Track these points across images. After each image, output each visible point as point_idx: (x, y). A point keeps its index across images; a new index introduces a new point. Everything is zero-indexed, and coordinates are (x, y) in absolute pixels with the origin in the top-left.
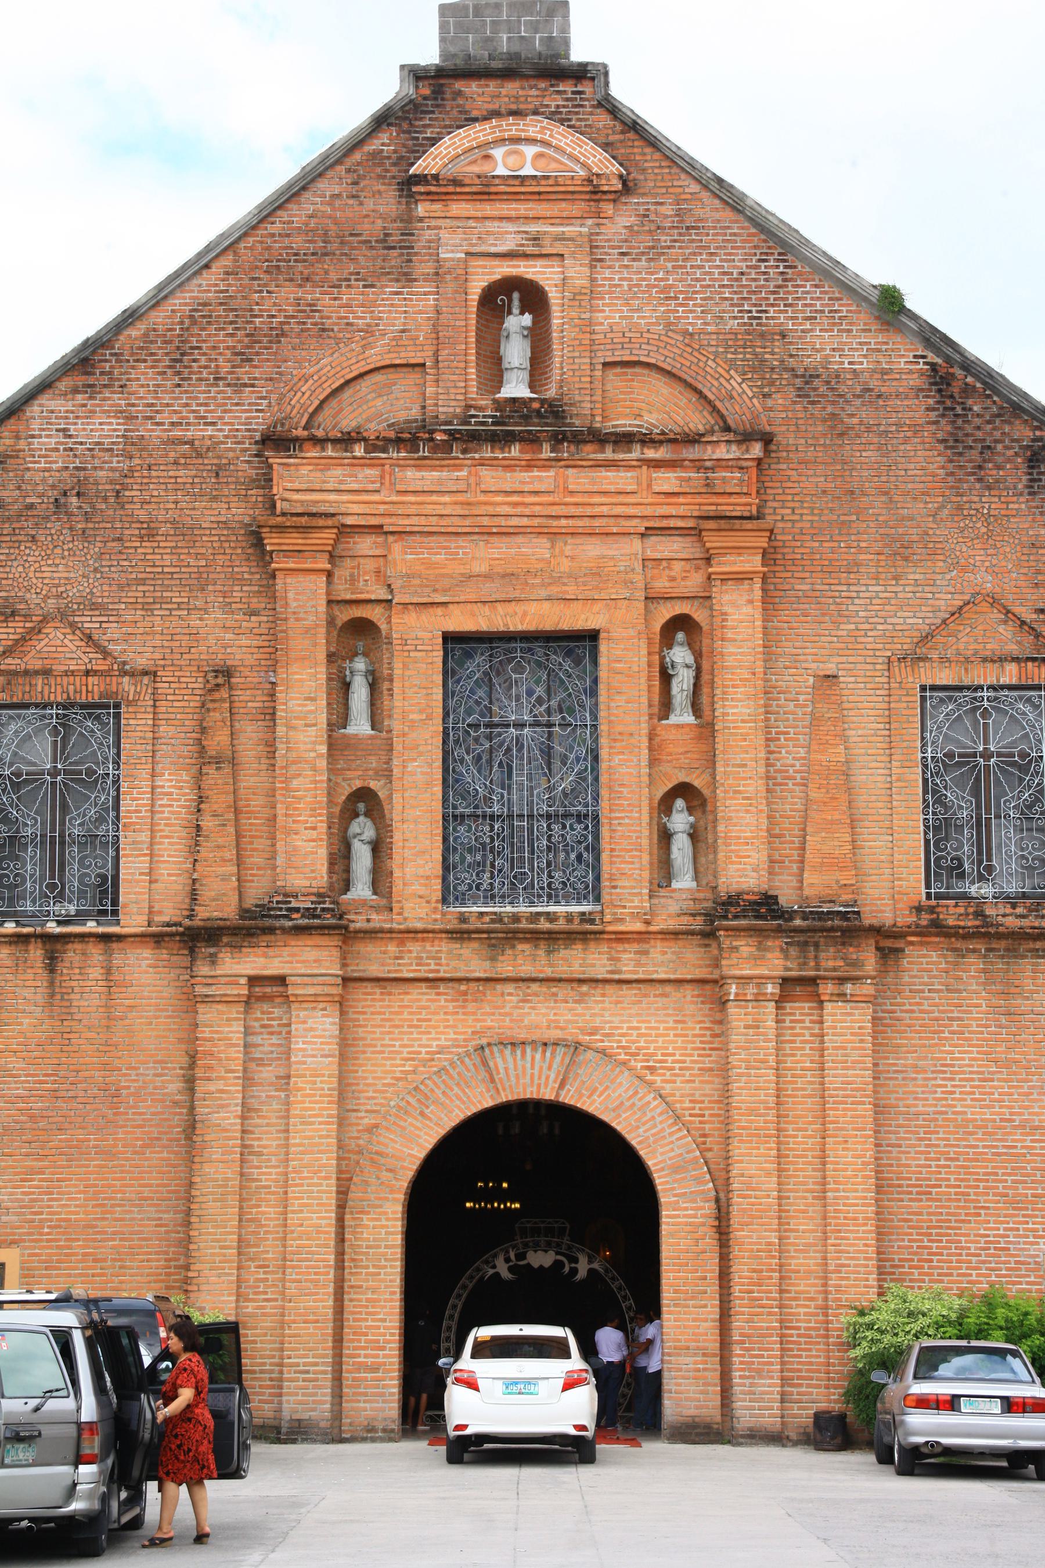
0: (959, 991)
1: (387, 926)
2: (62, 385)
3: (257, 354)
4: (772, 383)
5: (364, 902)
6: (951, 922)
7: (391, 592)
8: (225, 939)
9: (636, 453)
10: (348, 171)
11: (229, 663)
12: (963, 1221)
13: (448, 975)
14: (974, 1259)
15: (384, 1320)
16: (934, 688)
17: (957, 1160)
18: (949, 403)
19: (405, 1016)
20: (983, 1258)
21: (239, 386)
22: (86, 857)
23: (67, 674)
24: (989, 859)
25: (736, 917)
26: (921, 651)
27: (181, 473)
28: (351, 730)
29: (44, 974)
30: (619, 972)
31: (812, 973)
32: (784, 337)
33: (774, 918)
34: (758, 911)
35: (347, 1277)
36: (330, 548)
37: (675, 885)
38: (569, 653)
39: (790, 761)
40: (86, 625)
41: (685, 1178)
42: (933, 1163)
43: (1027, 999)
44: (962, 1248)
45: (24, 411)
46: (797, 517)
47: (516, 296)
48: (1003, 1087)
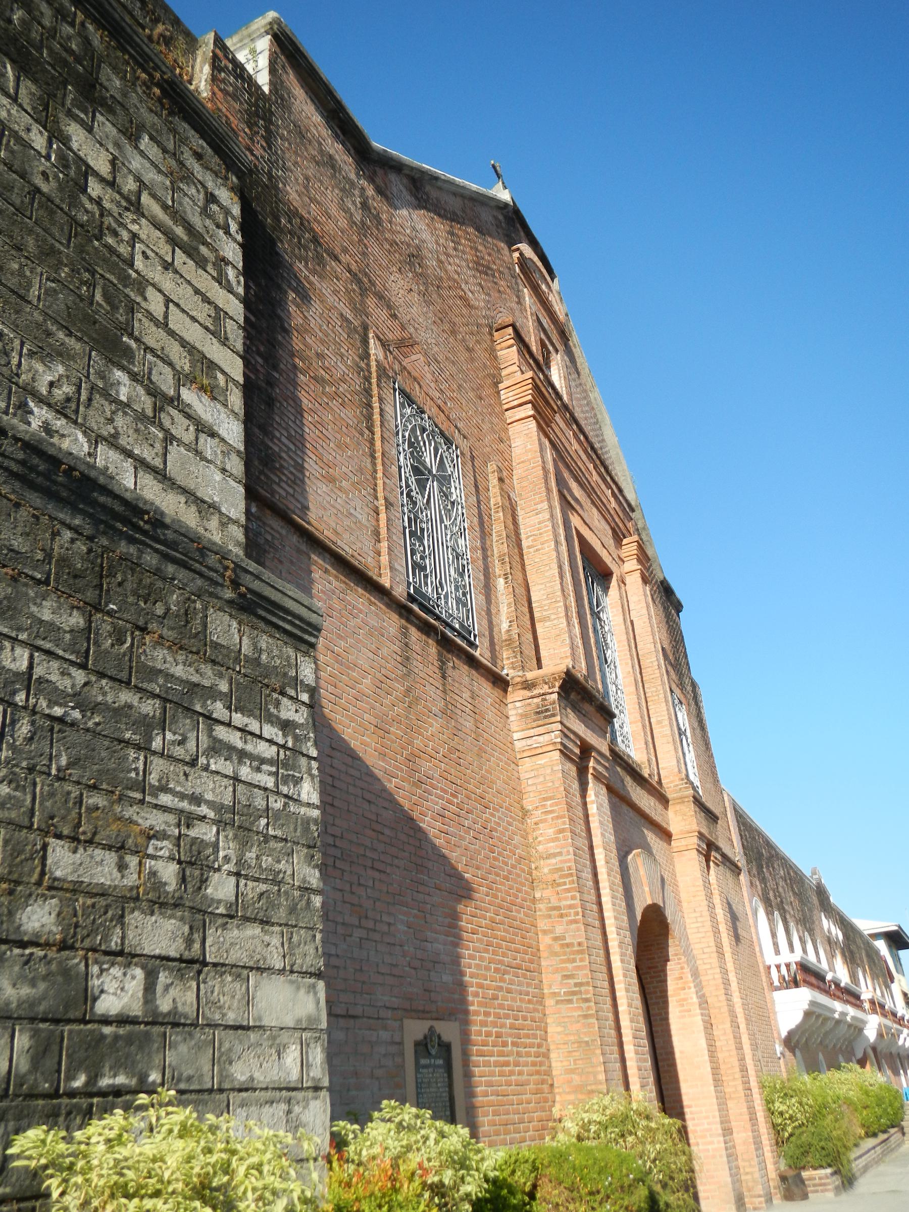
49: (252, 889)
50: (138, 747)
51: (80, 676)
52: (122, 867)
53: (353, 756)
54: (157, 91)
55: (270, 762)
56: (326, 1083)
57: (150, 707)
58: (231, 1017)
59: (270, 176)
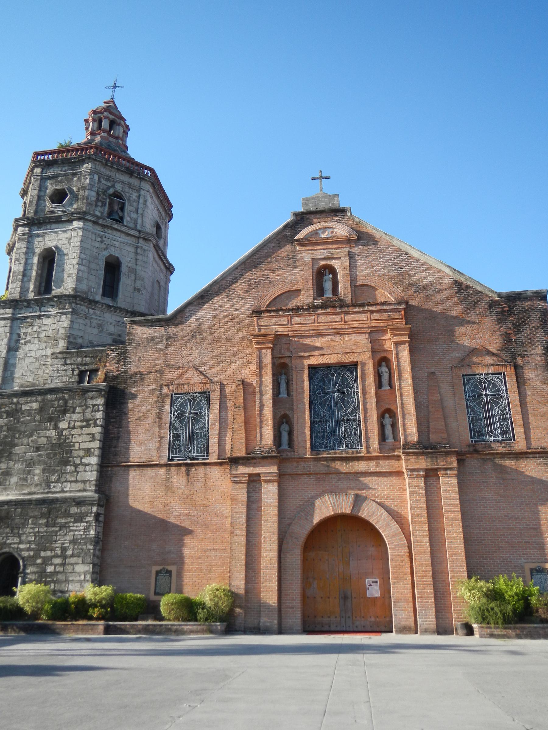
0: (484, 472)
1: (293, 457)
2: (195, 303)
3: (251, 290)
4: (407, 288)
5: (285, 451)
6: (480, 449)
7: (292, 354)
8: (240, 462)
9: (366, 308)
10: (277, 240)
11: (243, 378)
12: (494, 552)
13: (313, 472)
14: (499, 565)
15: (295, 590)
16: (467, 375)
17: (490, 530)
18: (462, 291)
19: (300, 486)
20: (502, 565)
21: (246, 299)
22: (199, 439)
23: (194, 384)
24: (491, 428)
25: (408, 449)
26: (462, 364)
27: (229, 324)
28: (280, 396)
29: (186, 476)
30: (370, 470)
31: (436, 467)
32: (409, 275)
33: (421, 449)
34: (416, 447)
35: (282, 575)
36: (272, 341)
37: (387, 441)
38: (348, 370)
39: (422, 400)
40: (200, 369)
41: (396, 539)
42: (482, 532)
43: (509, 474)
44: (495, 561)
45: (184, 311)
46: (417, 326)
47: (327, 270)
48: (503, 505)
49: (75, 552)
50: (55, 535)
51: (45, 529)
52: (51, 553)
53: (139, 511)
54: (81, 393)
55: (83, 530)
56: (90, 580)
57: (57, 529)
58: (70, 571)
59: (125, 371)
